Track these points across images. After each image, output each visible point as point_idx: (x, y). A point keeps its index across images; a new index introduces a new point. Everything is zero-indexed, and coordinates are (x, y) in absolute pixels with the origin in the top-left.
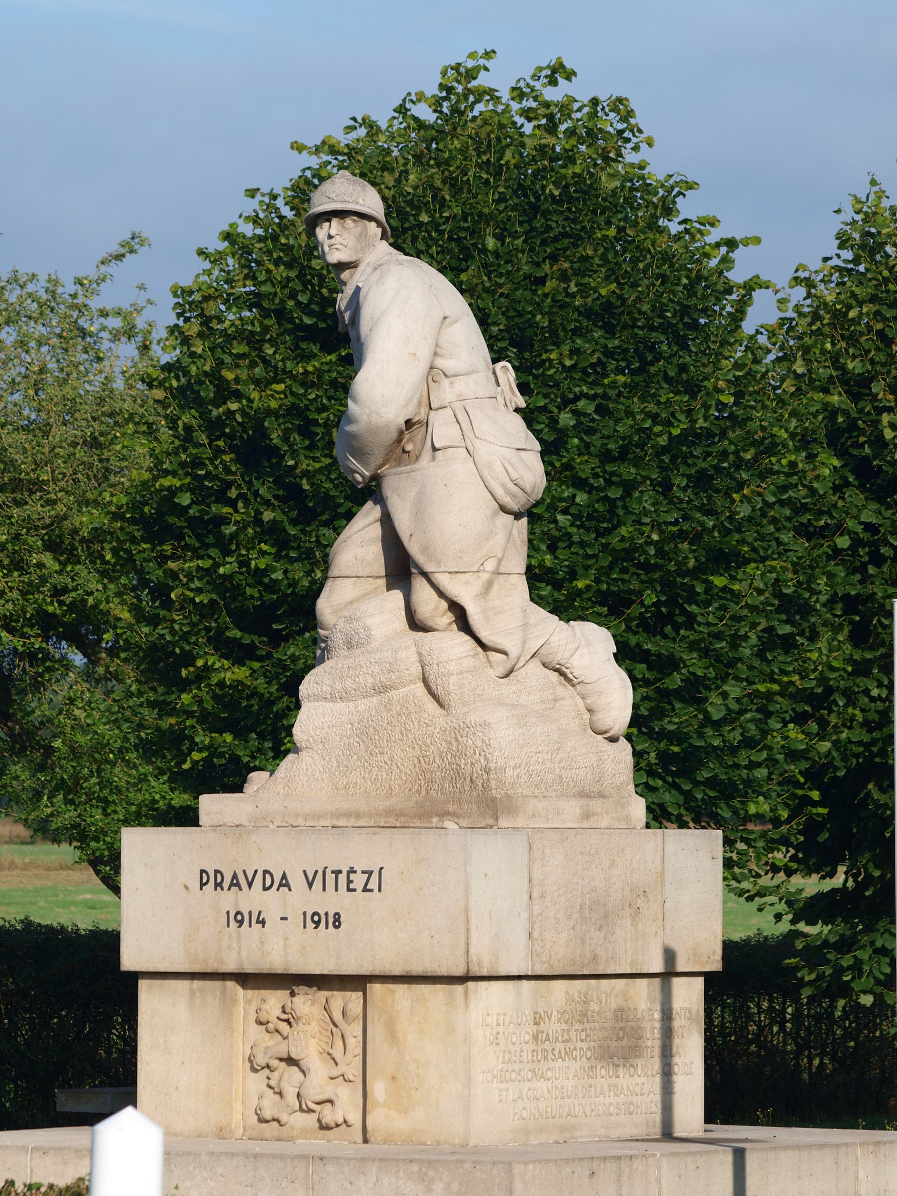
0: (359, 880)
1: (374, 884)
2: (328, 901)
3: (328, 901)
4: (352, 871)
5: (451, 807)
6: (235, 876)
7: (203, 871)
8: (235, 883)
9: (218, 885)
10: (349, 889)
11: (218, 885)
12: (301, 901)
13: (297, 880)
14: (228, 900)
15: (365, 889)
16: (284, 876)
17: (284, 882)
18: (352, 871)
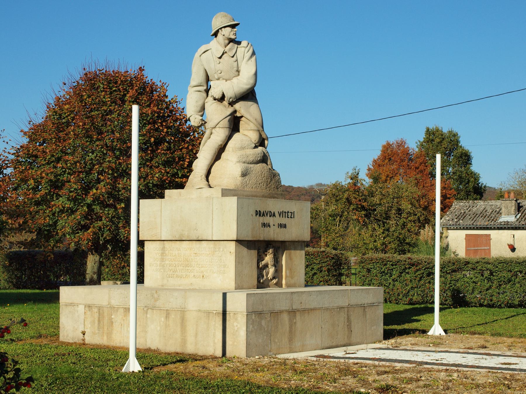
0: (290, 214)
1: (292, 216)
2: (284, 221)
3: (284, 221)
4: (288, 212)
5: (276, 196)
6: (263, 212)
7: (256, 211)
8: (263, 215)
9: (260, 215)
10: (288, 217)
11: (260, 215)
12: (278, 220)
13: (277, 214)
14: (262, 219)
15: (291, 217)
16: (274, 213)
17: (274, 215)
18: (288, 212)
